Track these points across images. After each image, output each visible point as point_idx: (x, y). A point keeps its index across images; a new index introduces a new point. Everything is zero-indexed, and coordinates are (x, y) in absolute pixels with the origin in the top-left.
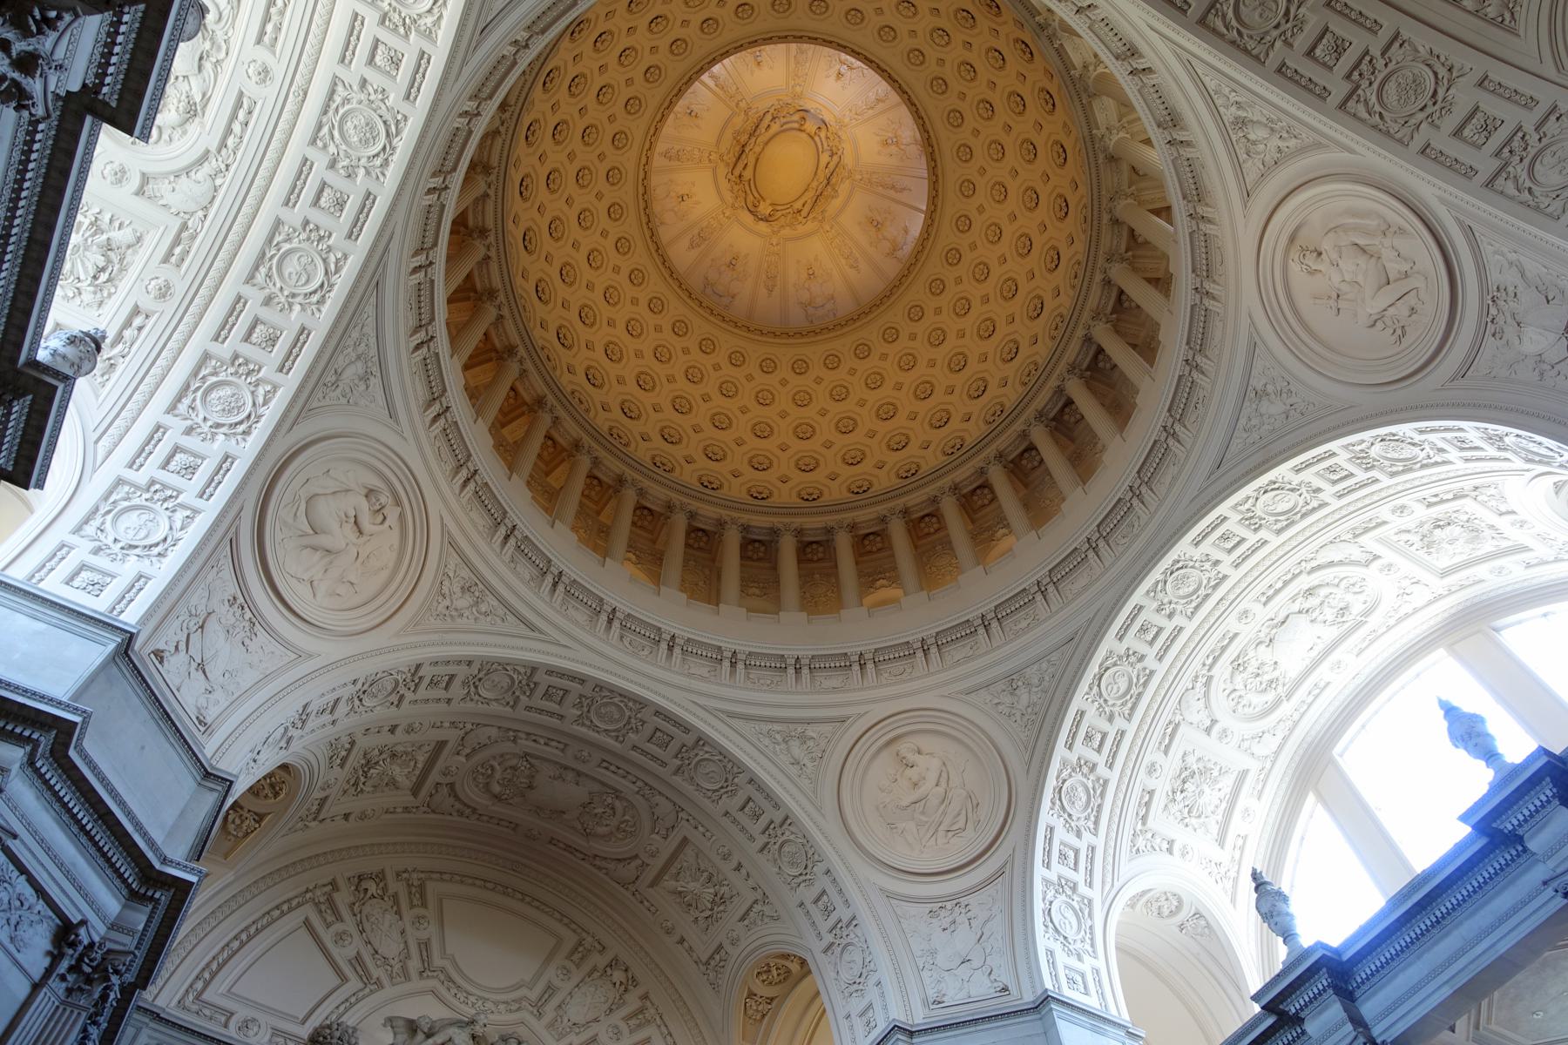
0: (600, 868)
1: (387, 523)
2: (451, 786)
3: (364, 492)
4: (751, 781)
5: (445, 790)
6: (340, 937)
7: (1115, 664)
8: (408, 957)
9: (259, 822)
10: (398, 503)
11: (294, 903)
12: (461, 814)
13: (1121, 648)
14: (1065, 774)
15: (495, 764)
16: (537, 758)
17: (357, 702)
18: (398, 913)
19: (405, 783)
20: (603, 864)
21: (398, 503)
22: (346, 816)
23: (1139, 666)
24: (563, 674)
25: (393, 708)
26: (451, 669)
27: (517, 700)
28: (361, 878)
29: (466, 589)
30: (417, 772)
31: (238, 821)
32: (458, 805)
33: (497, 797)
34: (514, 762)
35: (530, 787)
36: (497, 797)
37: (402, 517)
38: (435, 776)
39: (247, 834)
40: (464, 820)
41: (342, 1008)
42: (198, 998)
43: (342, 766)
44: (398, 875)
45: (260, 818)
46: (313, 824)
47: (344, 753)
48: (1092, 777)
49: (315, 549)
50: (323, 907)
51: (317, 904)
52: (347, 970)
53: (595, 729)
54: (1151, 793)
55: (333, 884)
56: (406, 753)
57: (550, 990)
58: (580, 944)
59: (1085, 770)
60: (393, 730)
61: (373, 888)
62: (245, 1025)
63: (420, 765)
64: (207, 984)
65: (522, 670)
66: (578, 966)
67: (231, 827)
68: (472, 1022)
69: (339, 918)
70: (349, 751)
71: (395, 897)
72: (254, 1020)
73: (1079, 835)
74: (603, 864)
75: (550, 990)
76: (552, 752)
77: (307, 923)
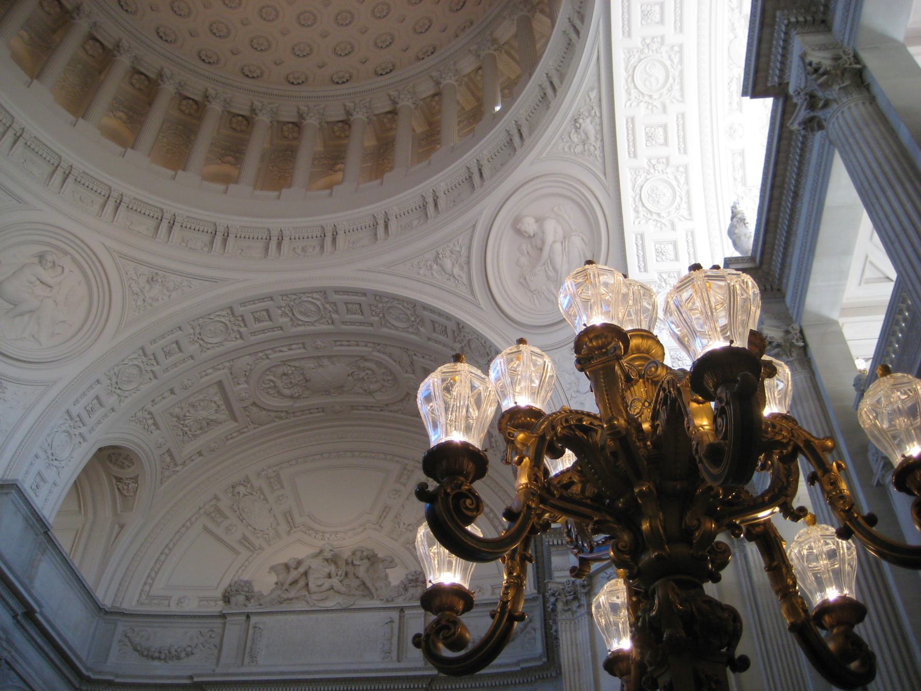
0: (397, 411)
1: (66, 270)
2: (254, 404)
3: (36, 260)
4: (424, 308)
5: (254, 409)
6: (228, 530)
7: (640, 60)
8: (278, 524)
9: (136, 482)
10: (66, 253)
11: (193, 519)
12: (281, 418)
13: (636, 41)
14: (640, 181)
15: (271, 378)
16: (294, 360)
17: (118, 391)
18: (265, 499)
19: (223, 416)
20: (395, 408)
21: (66, 253)
22: (200, 454)
23: (664, 49)
24: (253, 301)
25: (154, 382)
26: (172, 337)
27: (239, 332)
28: (233, 487)
29: (151, 280)
30: (223, 407)
31: (126, 487)
32: (273, 414)
33: (292, 397)
34: (281, 370)
35: (307, 381)
36: (292, 397)
37: (74, 260)
38: (236, 406)
39: (135, 492)
40: (287, 421)
41: (240, 571)
42: (148, 596)
43: (158, 428)
44: (259, 474)
45: (135, 479)
46: (177, 469)
47: (151, 422)
48: (669, 170)
49: (22, 314)
50: (213, 515)
51: (208, 514)
52: (238, 547)
53: (305, 323)
54: (742, 153)
55: (216, 498)
56: (203, 401)
57: (386, 509)
58: (405, 469)
59: (660, 167)
60: (172, 392)
61: (242, 490)
62: (179, 602)
63: (221, 403)
64: (151, 586)
65: (224, 313)
66: (404, 485)
67: (125, 492)
68: (321, 552)
69: (226, 517)
70: (153, 418)
71: (260, 489)
72: (184, 597)
73: (673, 227)
74: (395, 408)
75: (386, 509)
76: (298, 352)
77: (206, 529)
